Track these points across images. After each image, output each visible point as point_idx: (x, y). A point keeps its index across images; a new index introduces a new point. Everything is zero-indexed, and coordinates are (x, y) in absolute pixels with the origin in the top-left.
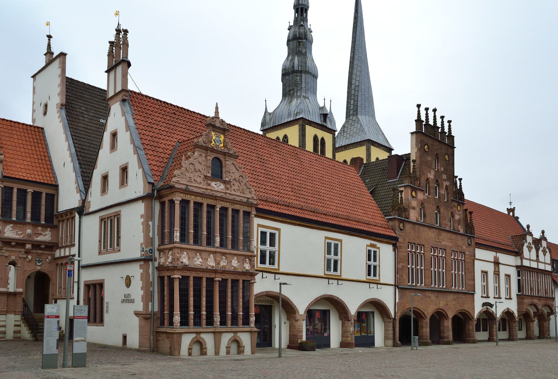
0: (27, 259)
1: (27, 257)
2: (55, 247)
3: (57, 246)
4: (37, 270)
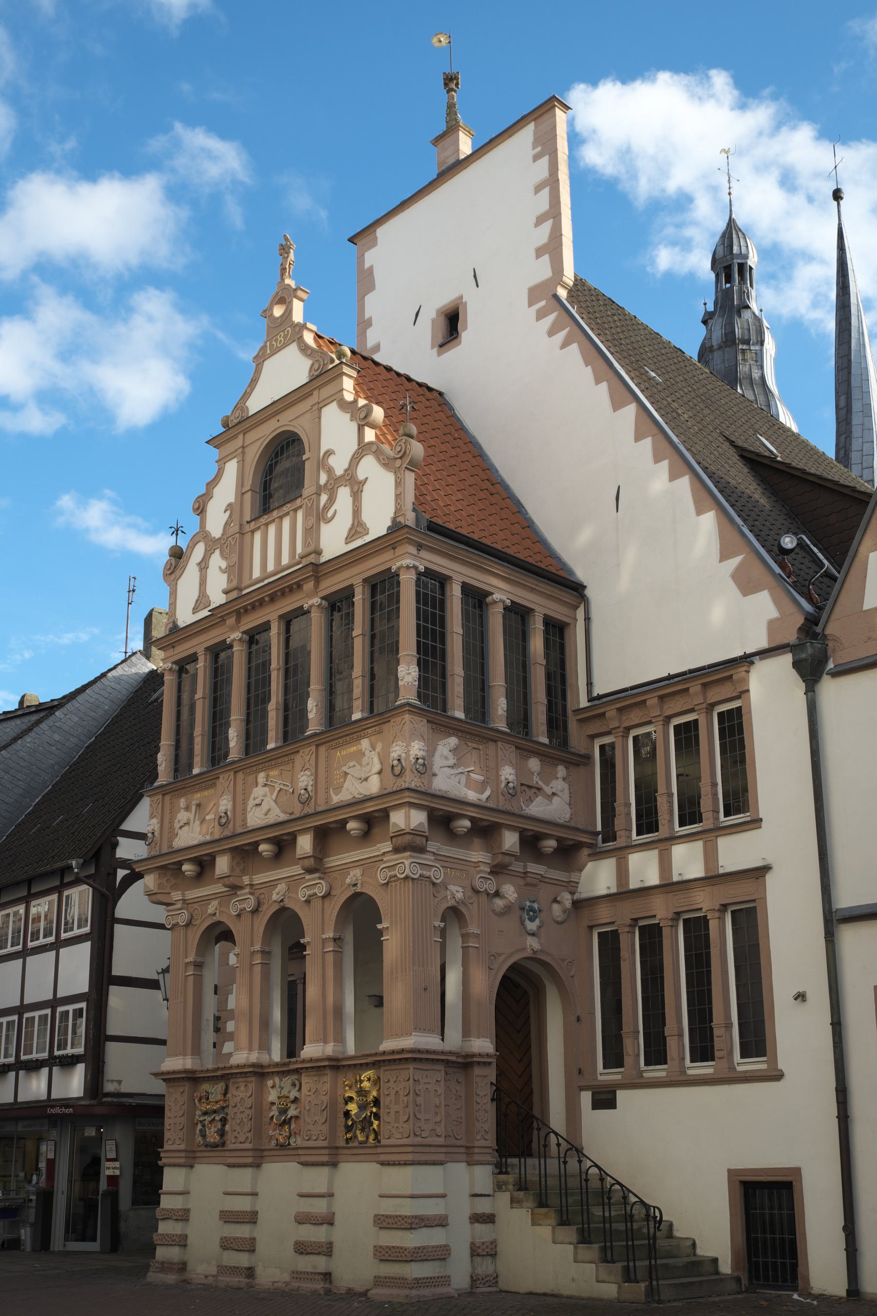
0: (499, 903)
1: (497, 894)
2: (585, 852)
3: (591, 846)
4: (528, 953)
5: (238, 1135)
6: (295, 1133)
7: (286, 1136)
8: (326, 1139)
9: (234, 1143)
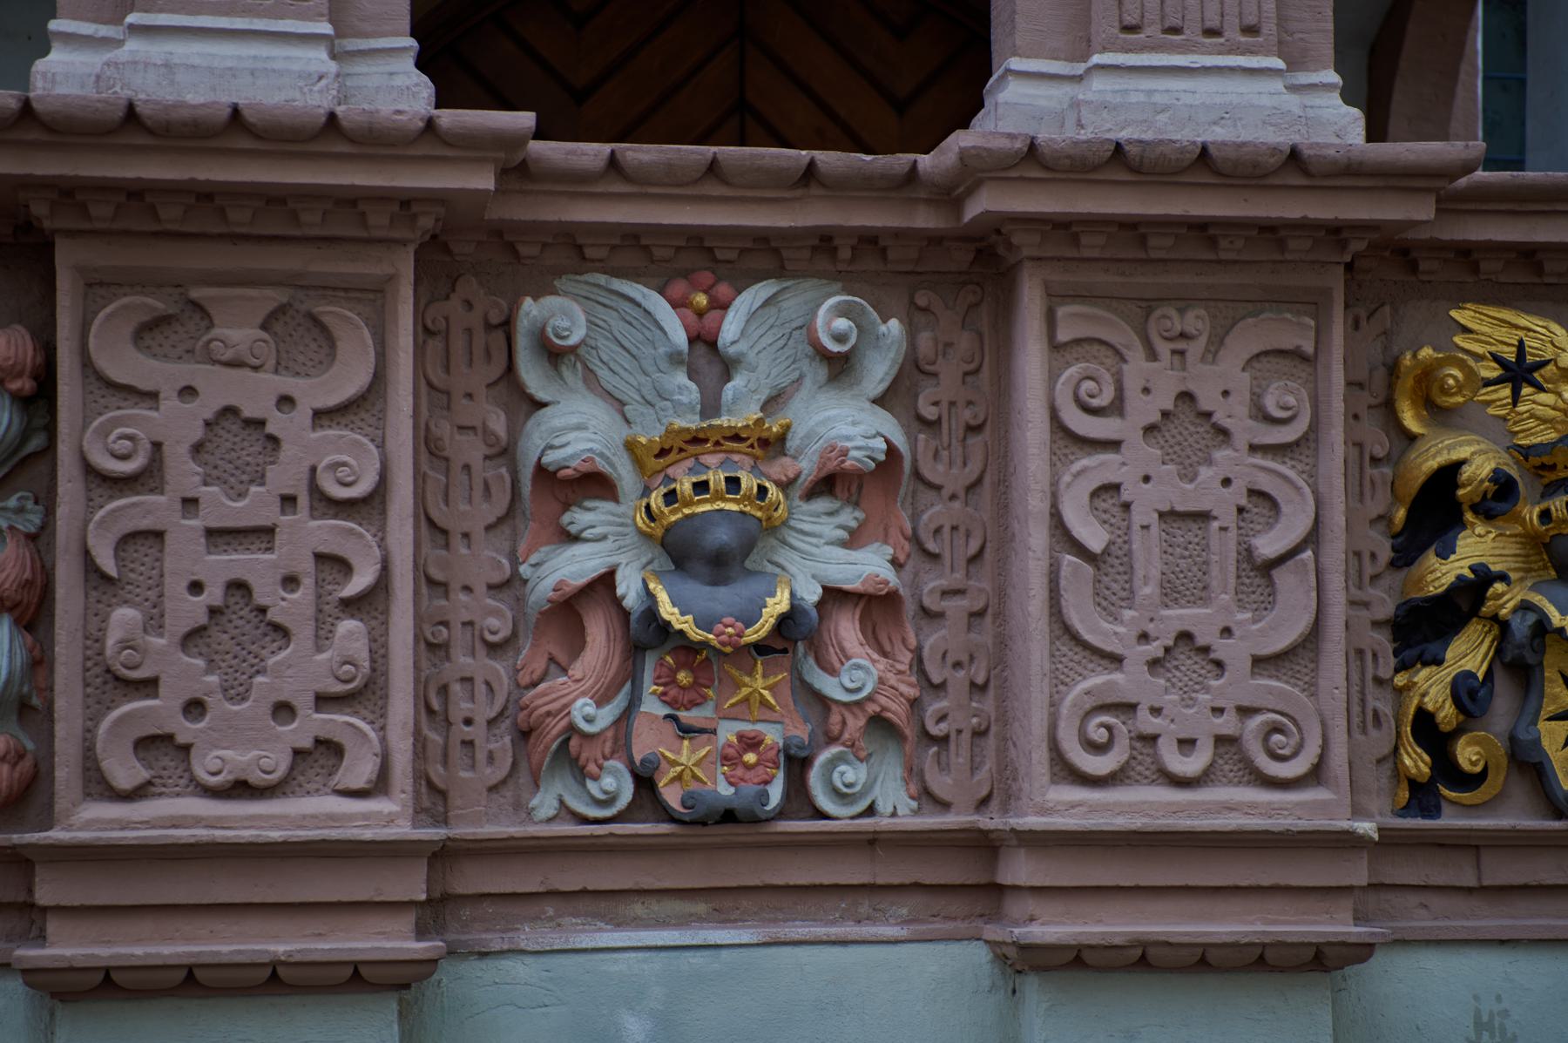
5: (186, 730)
6: (880, 724)
7: (751, 743)
8: (1316, 775)
9: (138, 793)
